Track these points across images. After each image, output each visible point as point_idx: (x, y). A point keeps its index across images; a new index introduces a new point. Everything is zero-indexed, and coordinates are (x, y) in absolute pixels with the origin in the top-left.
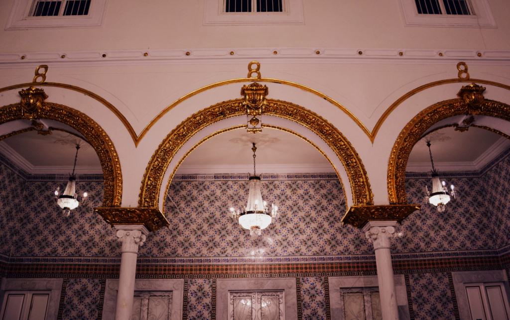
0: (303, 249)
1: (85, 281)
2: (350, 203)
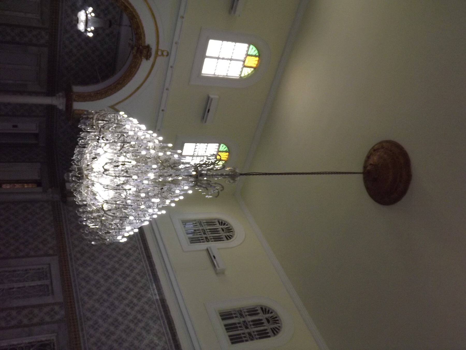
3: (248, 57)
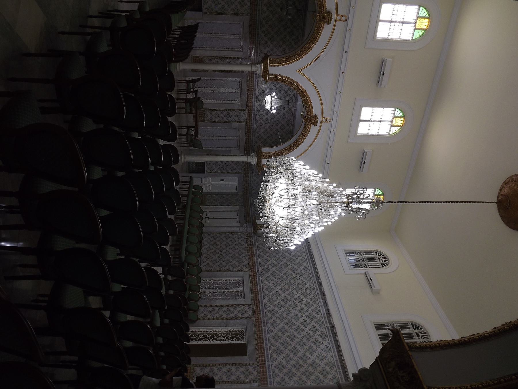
0: (259, 114)
1: (249, 4)
2: (265, 150)
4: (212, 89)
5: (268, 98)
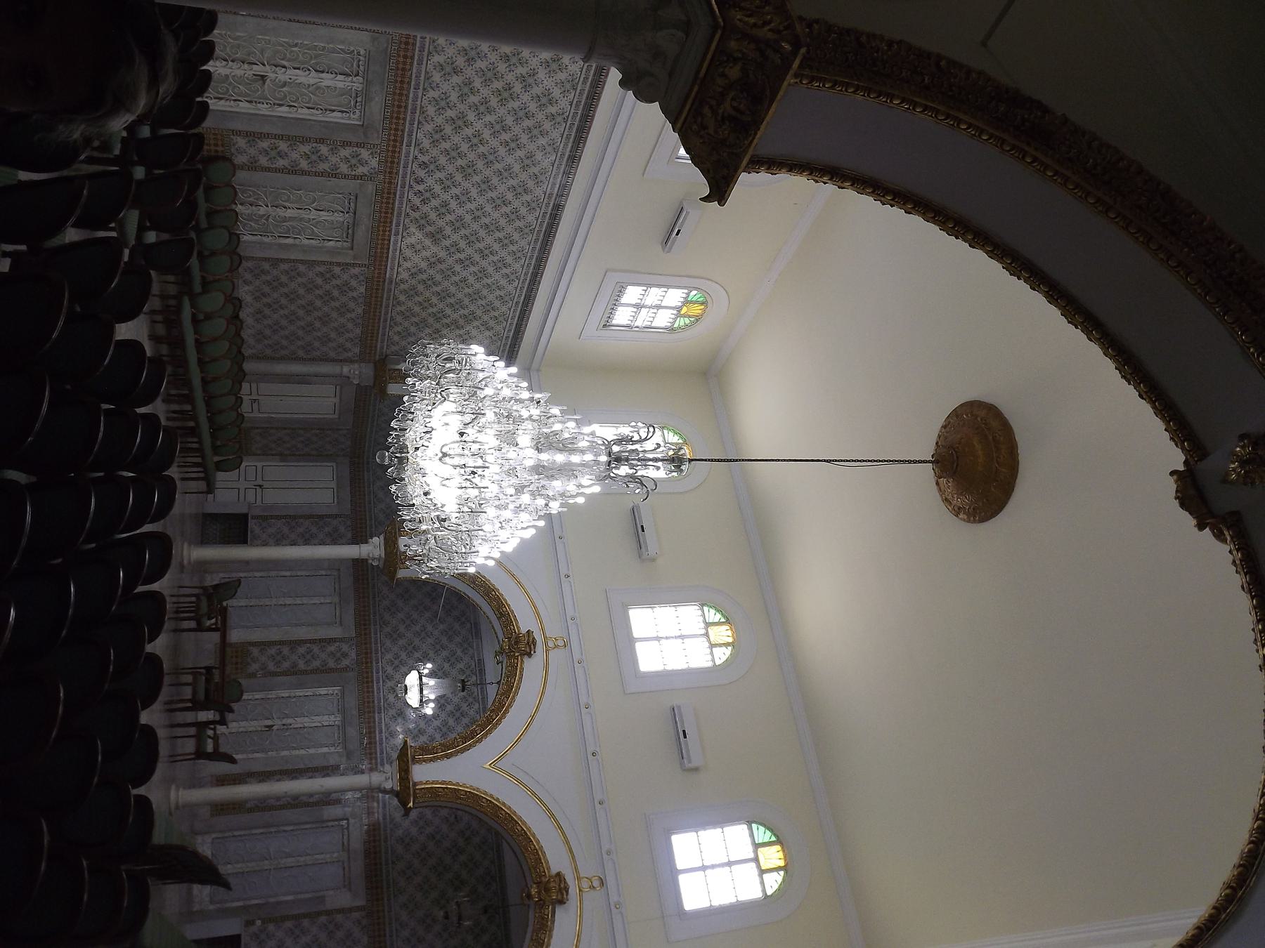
3: (761, 850)
4: (269, 723)
5: (412, 679)
